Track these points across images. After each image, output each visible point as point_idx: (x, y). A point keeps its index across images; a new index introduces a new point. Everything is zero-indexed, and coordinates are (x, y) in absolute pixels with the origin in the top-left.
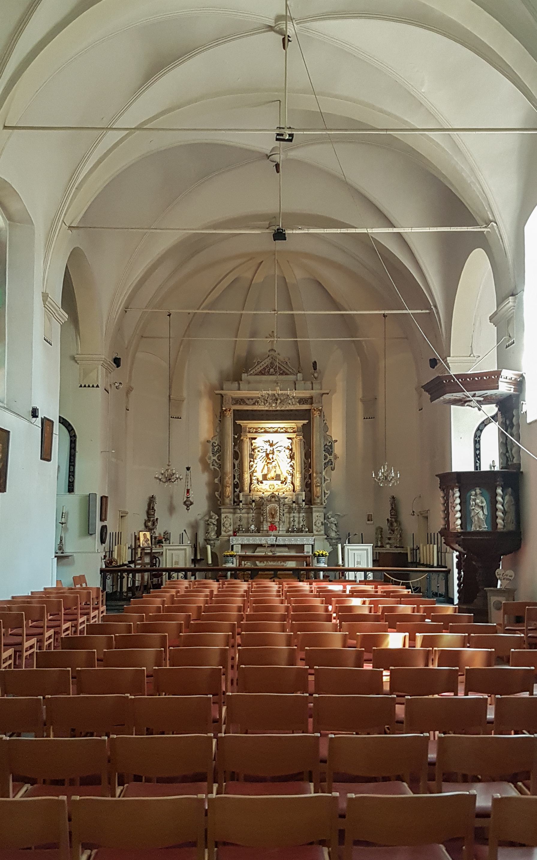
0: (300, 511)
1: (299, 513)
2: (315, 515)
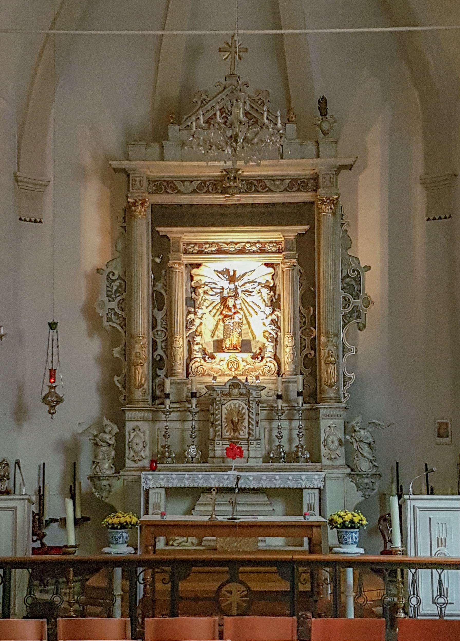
0: (294, 415)
1: (291, 420)
2: (324, 423)
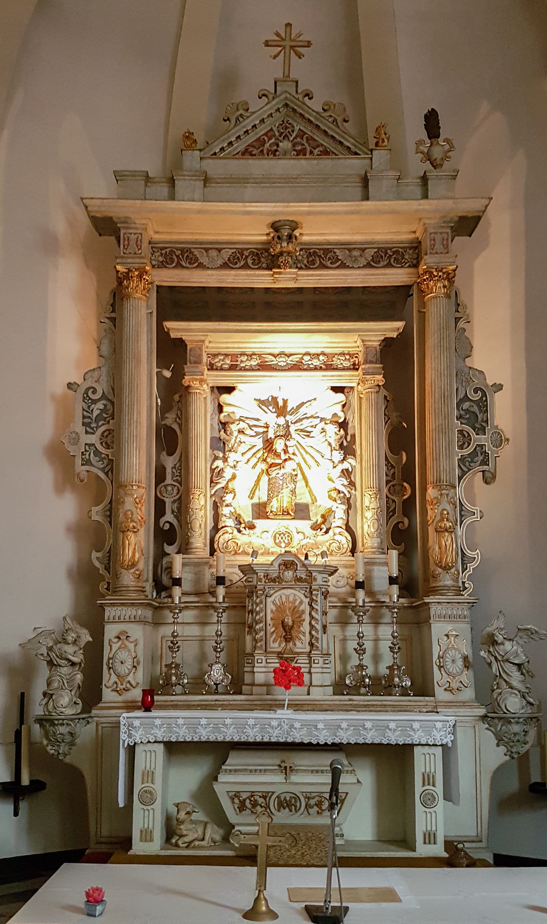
0: (381, 616)
1: (376, 622)
